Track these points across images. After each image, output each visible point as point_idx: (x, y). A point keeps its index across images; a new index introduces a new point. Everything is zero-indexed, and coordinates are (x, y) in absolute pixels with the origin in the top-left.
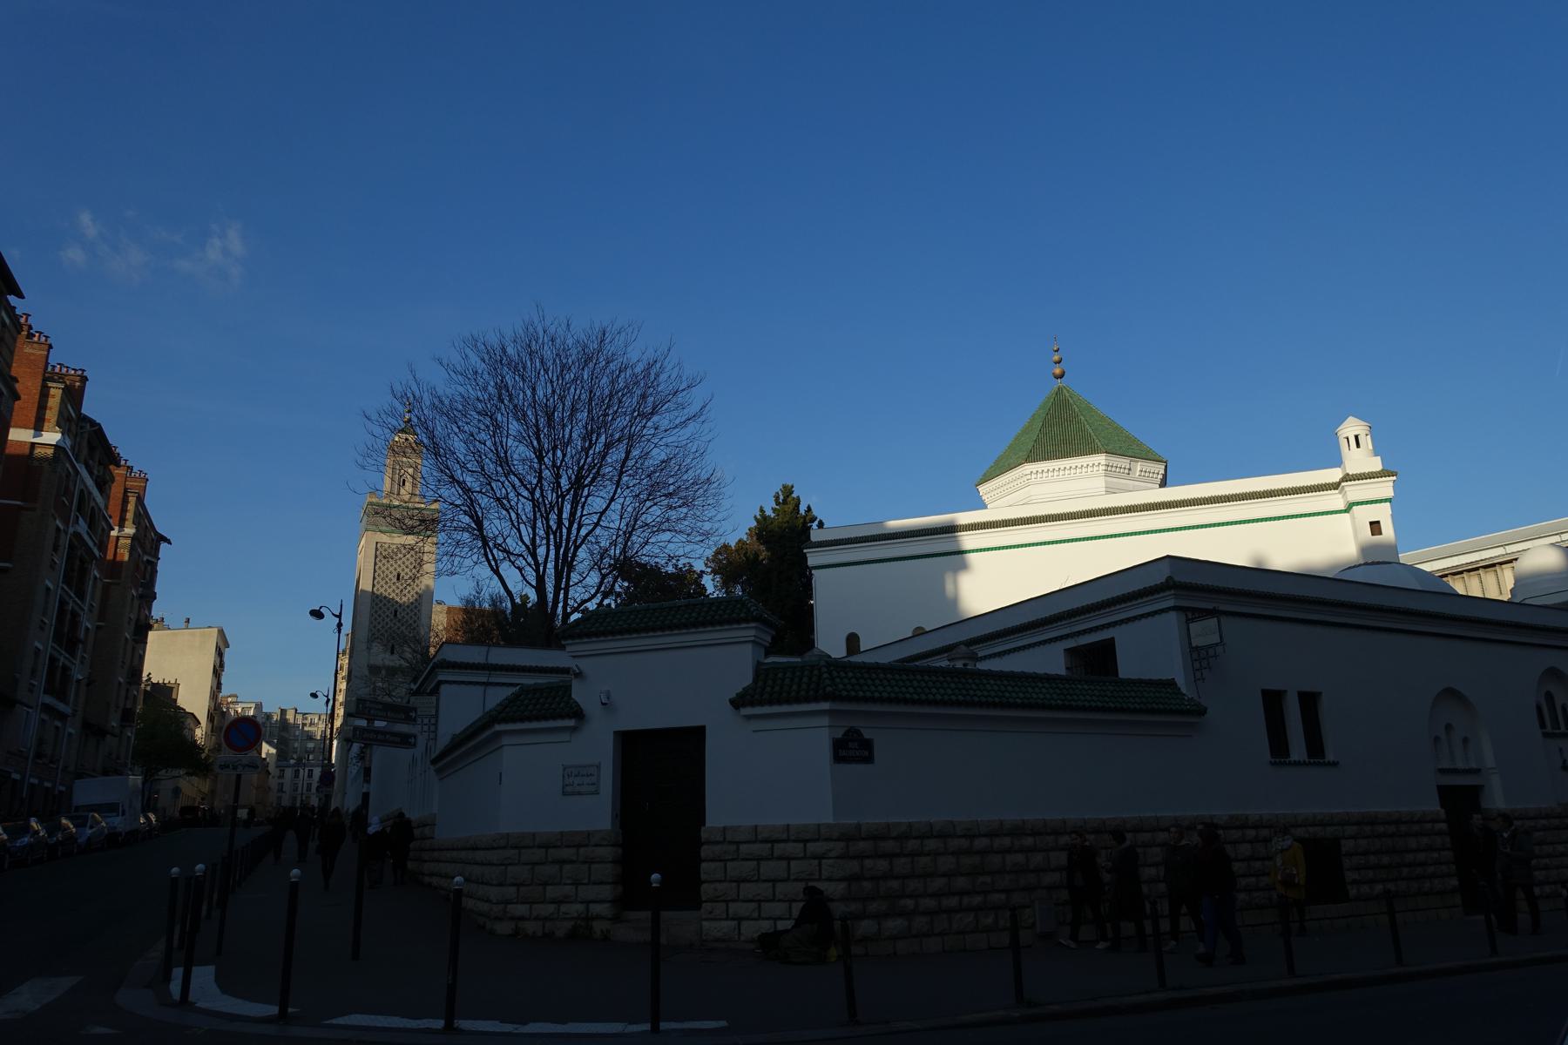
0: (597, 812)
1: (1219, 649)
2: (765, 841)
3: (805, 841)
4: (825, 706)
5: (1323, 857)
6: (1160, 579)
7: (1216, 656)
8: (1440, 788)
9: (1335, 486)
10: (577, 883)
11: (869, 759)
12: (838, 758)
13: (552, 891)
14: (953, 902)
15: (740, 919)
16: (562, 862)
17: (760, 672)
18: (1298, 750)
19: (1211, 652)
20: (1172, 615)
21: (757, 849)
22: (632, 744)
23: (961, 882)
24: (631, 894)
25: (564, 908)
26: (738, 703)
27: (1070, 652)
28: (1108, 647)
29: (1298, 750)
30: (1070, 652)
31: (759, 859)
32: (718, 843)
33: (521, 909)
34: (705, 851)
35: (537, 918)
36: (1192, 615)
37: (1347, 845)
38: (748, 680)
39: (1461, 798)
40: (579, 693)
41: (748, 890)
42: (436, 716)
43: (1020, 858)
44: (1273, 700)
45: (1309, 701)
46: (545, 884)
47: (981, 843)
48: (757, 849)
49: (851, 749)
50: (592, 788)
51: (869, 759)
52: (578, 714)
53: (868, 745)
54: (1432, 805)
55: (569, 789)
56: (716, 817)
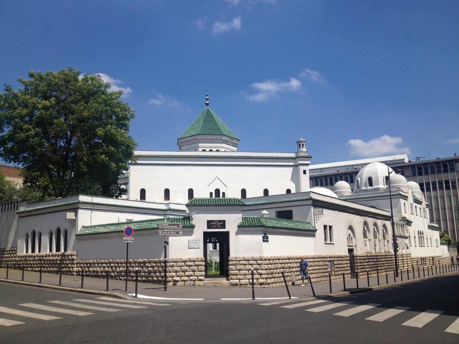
0: (198, 254)
1: (322, 216)
2: (246, 260)
3: (256, 261)
4: (262, 229)
7: (321, 217)
10: (194, 271)
11: (267, 241)
12: (264, 241)
13: (187, 273)
15: (240, 279)
16: (189, 266)
17: (244, 219)
19: (320, 216)
21: (243, 262)
25: (191, 278)
27: (276, 211)
28: (291, 211)
30: (276, 211)
31: (245, 265)
32: (234, 261)
34: (230, 263)
35: (182, 281)
38: (241, 221)
39: (351, 251)
41: (243, 272)
43: (289, 265)
44: (325, 227)
45: (331, 227)
46: (184, 272)
47: (284, 261)
48: (243, 262)
50: (198, 247)
51: (267, 241)
53: (267, 237)
54: (346, 253)
55: (190, 247)
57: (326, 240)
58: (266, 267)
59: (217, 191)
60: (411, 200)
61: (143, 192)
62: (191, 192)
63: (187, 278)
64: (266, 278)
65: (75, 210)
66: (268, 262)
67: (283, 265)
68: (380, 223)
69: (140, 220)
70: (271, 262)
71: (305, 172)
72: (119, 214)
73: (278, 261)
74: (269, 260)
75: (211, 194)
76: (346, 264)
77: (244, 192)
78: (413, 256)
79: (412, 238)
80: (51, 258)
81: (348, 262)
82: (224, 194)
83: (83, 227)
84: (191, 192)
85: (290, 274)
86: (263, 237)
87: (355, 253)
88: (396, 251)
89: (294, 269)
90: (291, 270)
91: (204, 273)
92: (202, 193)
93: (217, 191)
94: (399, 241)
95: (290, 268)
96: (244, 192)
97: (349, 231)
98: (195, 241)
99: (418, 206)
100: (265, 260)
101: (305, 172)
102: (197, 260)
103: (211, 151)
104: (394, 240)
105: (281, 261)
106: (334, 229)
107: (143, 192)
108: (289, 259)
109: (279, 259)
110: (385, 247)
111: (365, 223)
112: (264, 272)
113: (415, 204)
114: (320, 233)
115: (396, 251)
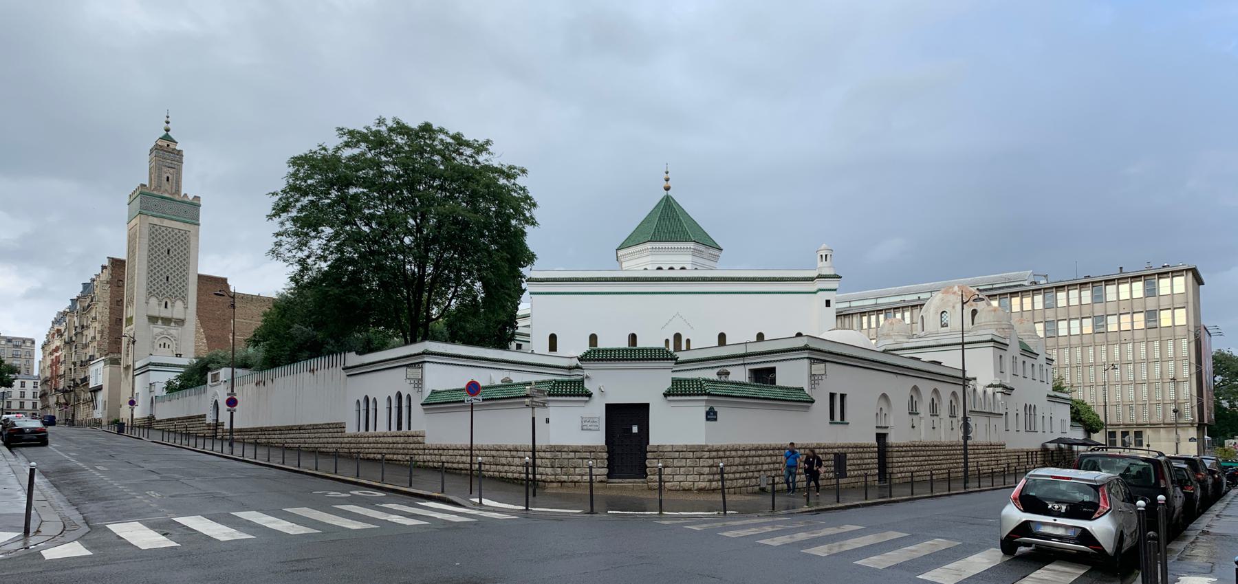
0: (598, 438)
5: (840, 460)
6: (800, 343)
8: (878, 435)
9: (812, 279)
12: (708, 419)
14: (738, 475)
17: (676, 382)
18: (837, 418)
20: (806, 361)
22: (614, 411)
23: (741, 468)
24: (614, 470)
26: (665, 395)
28: (773, 370)
29: (837, 418)
33: (565, 478)
34: (649, 455)
36: (814, 361)
37: (849, 456)
39: (881, 437)
40: (588, 386)
42: (422, 379)
44: (832, 396)
45: (843, 396)
47: (747, 453)
49: (711, 415)
52: (590, 395)
53: (715, 413)
54: (873, 441)
56: (654, 440)
57: (832, 417)
58: (711, 462)
59: (678, 337)
60: (1014, 349)
61: (553, 338)
62: (593, 339)
63: (579, 478)
64: (710, 481)
65: (419, 365)
66: (714, 454)
67: (743, 460)
68: (946, 391)
69: (520, 381)
70: (721, 454)
71: (828, 303)
72: (493, 373)
73: (733, 453)
74: (717, 451)
75: (667, 341)
76: (872, 460)
77: (633, 338)
78: (1008, 447)
79: (1012, 417)
80: (390, 440)
81: (875, 455)
82: (688, 341)
83: (433, 392)
84: (593, 339)
85: (756, 474)
86: (708, 413)
87: (892, 439)
88: (966, 438)
89: (765, 467)
90: (759, 467)
91: (605, 471)
92: (613, 340)
93: (678, 337)
94: (972, 423)
95: (757, 464)
96: (633, 338)
97: (883, 405)
98: (592, 420)
99: (1029, 361)
100: (710, 451)
101: (828, 303)
102: (591, 450)
103: (671, 268)
104: (965, 419)
105: (740, 453)
106: (848, 400)
107: (553, 338)
108: (756, 449)
109: (736, 450)
110: (947, 432)
111: (915, 388)
112: (707, 470)
113: (1021, 359)
114: (822, 404)
115: (966, 438)
